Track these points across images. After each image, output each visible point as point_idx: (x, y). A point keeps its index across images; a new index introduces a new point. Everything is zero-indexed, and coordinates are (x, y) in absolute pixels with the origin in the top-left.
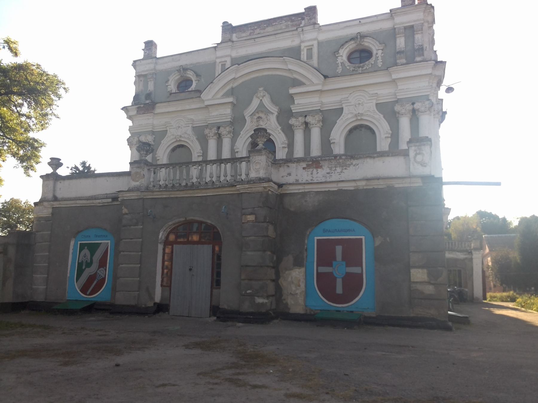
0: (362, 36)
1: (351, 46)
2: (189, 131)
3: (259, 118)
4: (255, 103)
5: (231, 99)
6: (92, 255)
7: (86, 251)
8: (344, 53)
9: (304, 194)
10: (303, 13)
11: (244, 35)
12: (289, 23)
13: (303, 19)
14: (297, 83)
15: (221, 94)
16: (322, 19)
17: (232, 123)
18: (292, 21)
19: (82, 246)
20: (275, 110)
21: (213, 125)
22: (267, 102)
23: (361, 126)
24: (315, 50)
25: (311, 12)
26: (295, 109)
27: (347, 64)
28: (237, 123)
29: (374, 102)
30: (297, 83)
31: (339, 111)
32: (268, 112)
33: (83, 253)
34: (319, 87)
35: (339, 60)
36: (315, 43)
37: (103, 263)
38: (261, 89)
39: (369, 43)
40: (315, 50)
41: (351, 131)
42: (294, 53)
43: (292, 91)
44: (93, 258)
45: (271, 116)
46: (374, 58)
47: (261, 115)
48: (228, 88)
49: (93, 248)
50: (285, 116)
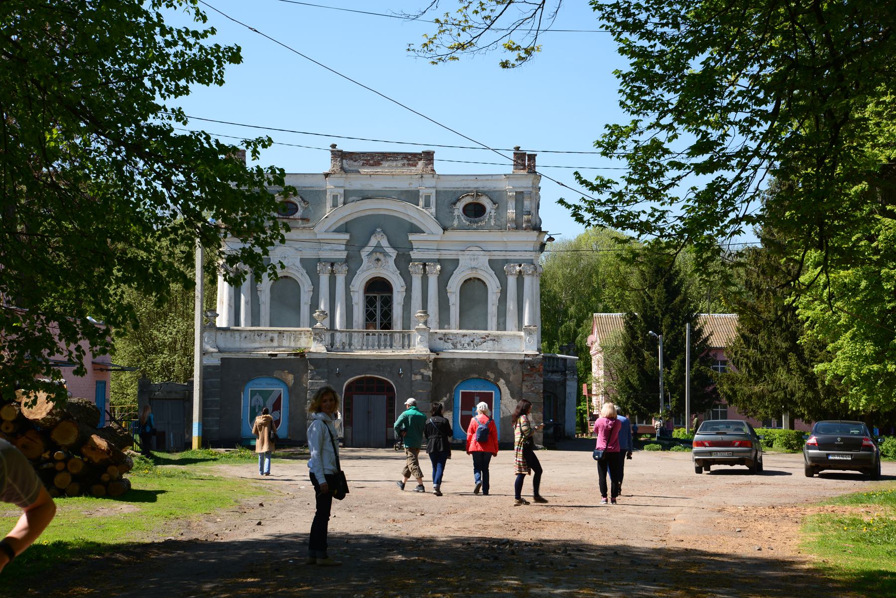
0: (478, 193)
1: (468, 200)
2: (298, 264)
3: (378, 260)
4: (373, 242)
5: (347, 236)
6: (265, 400)
7: (257, 397)
8: (460, 205)
9: (453, 360)
10: (420, 154)
11: (356, 163)
12: (405, 162)
13: (420, 159)
14: (416, 230)
15: (334, 228)
16: (439, 167)
17: (346, 261)
18: (409, 160)
19: (253, 393)
20: (393, 253)
21: (326, 261)
22: (384, 243)
23: (475, 278)
24: (433, 199)
25: (428, 156)
26: (414, 255)
27: (463, 218)
28: (352, 262)
29: (488, 258)
30: (416, 230)
31: (456, 262)
32: (386, 254)
33: (255, 398)
34: (438, 238)
35: (456, 213)
36: (434, 191)
37: (277, 406)
38: (378, 230)
39: (485, 201)
40: (433, 199)
41: (466, 281)
42: (412, 196)
43: (412, 237)
44: (267, 402)
45: (389, 259)
46: (487, 215)
47: (379, 255)
48: (342, 222)
49: (265, 394)
50: (403, 262)
